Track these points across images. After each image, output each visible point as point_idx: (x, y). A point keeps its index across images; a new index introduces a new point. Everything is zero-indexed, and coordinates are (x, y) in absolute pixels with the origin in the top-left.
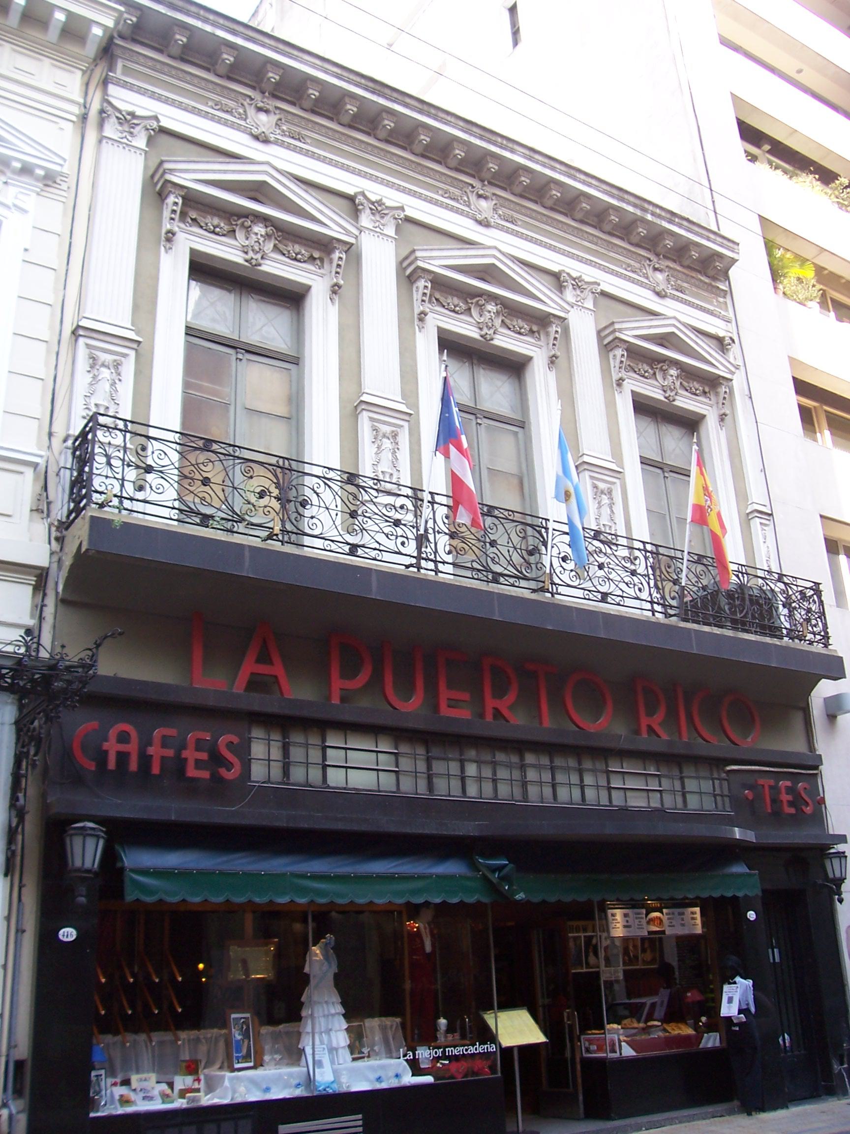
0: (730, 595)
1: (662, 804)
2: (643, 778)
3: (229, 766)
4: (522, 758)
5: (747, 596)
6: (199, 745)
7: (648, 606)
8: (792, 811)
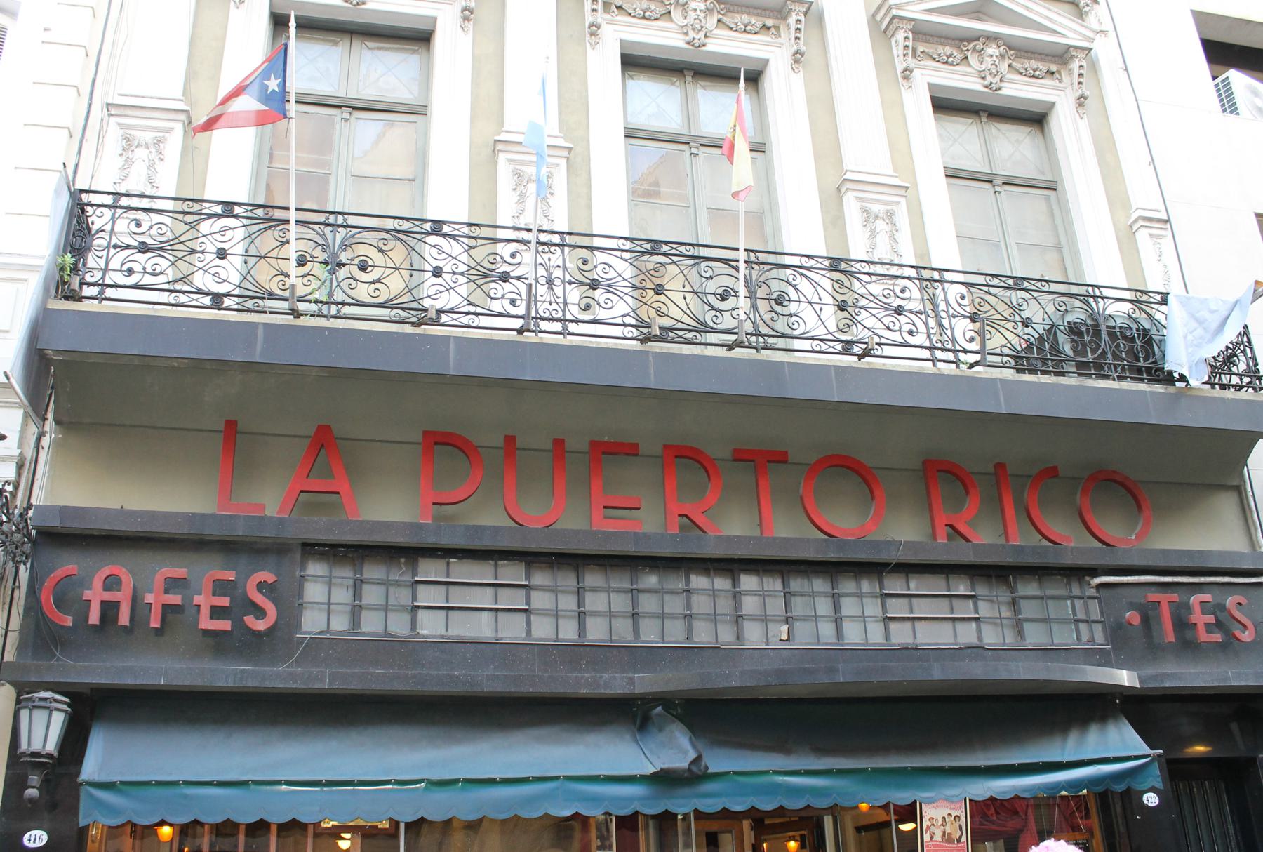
0: (1074, 330)
1: (980, 638)
2: (945, 602)
3: (260, 612)
4: (735, 582)
5: (1103, 329)
6: (221, 587)
7: (926, 354)
8: (1217, 637)
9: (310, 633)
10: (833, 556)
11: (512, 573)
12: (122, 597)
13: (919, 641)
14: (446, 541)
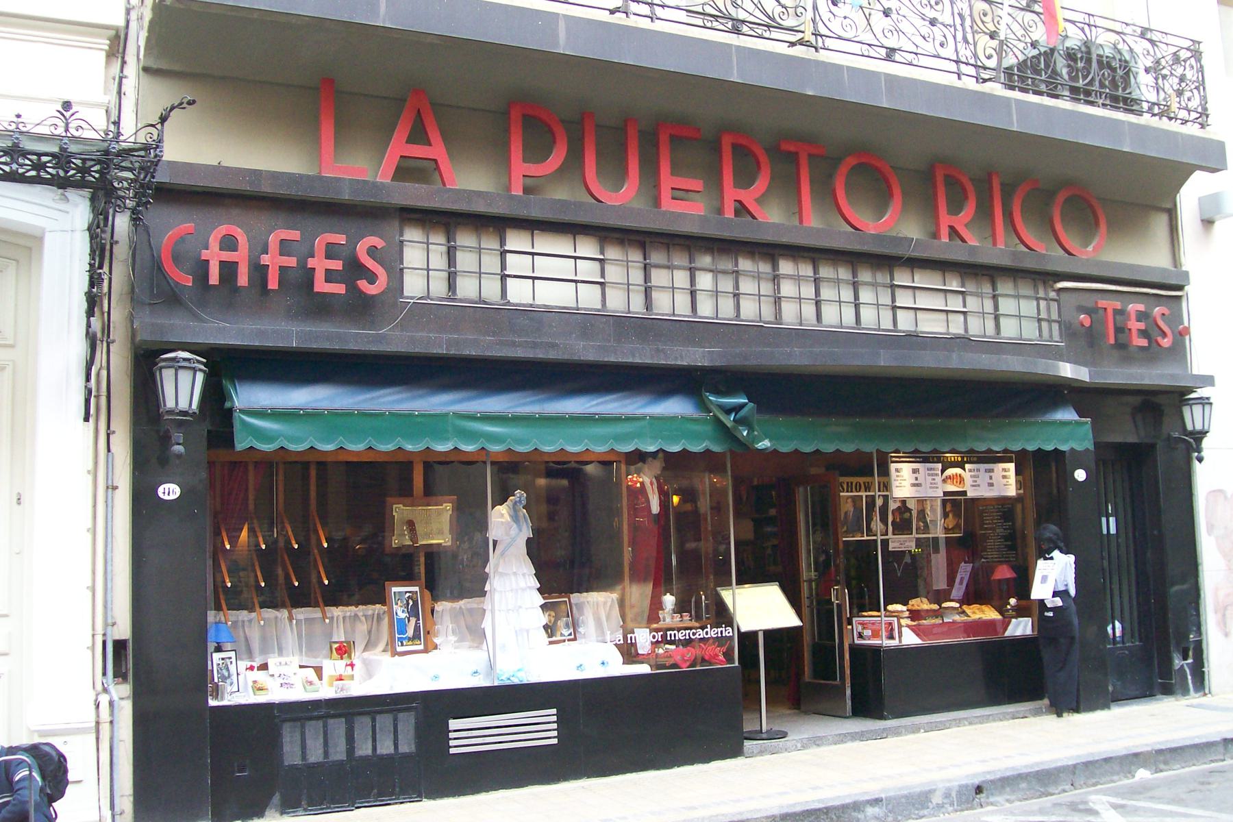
0: (1071, 56)
1: (966, 330)
2: (941, 295)
3: (372, 278)
4: (775, 267)
5: (1094, 57)
6: (331, 252)
7: (953, 67)
8: (1144, 342)
9: (412, 298)
10: (857, 247)
11: (587, 248)
12: (241, 256)
13: (920, 328)
14: (536, 213)
